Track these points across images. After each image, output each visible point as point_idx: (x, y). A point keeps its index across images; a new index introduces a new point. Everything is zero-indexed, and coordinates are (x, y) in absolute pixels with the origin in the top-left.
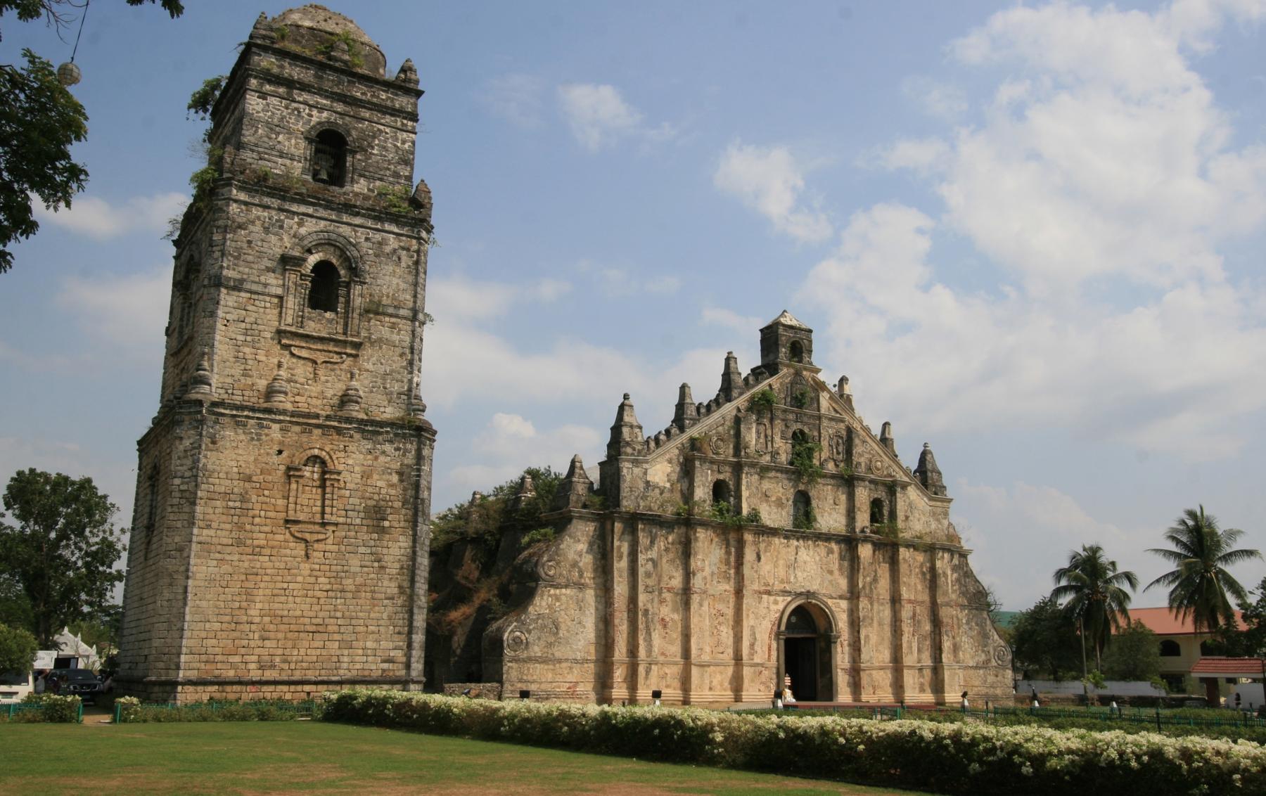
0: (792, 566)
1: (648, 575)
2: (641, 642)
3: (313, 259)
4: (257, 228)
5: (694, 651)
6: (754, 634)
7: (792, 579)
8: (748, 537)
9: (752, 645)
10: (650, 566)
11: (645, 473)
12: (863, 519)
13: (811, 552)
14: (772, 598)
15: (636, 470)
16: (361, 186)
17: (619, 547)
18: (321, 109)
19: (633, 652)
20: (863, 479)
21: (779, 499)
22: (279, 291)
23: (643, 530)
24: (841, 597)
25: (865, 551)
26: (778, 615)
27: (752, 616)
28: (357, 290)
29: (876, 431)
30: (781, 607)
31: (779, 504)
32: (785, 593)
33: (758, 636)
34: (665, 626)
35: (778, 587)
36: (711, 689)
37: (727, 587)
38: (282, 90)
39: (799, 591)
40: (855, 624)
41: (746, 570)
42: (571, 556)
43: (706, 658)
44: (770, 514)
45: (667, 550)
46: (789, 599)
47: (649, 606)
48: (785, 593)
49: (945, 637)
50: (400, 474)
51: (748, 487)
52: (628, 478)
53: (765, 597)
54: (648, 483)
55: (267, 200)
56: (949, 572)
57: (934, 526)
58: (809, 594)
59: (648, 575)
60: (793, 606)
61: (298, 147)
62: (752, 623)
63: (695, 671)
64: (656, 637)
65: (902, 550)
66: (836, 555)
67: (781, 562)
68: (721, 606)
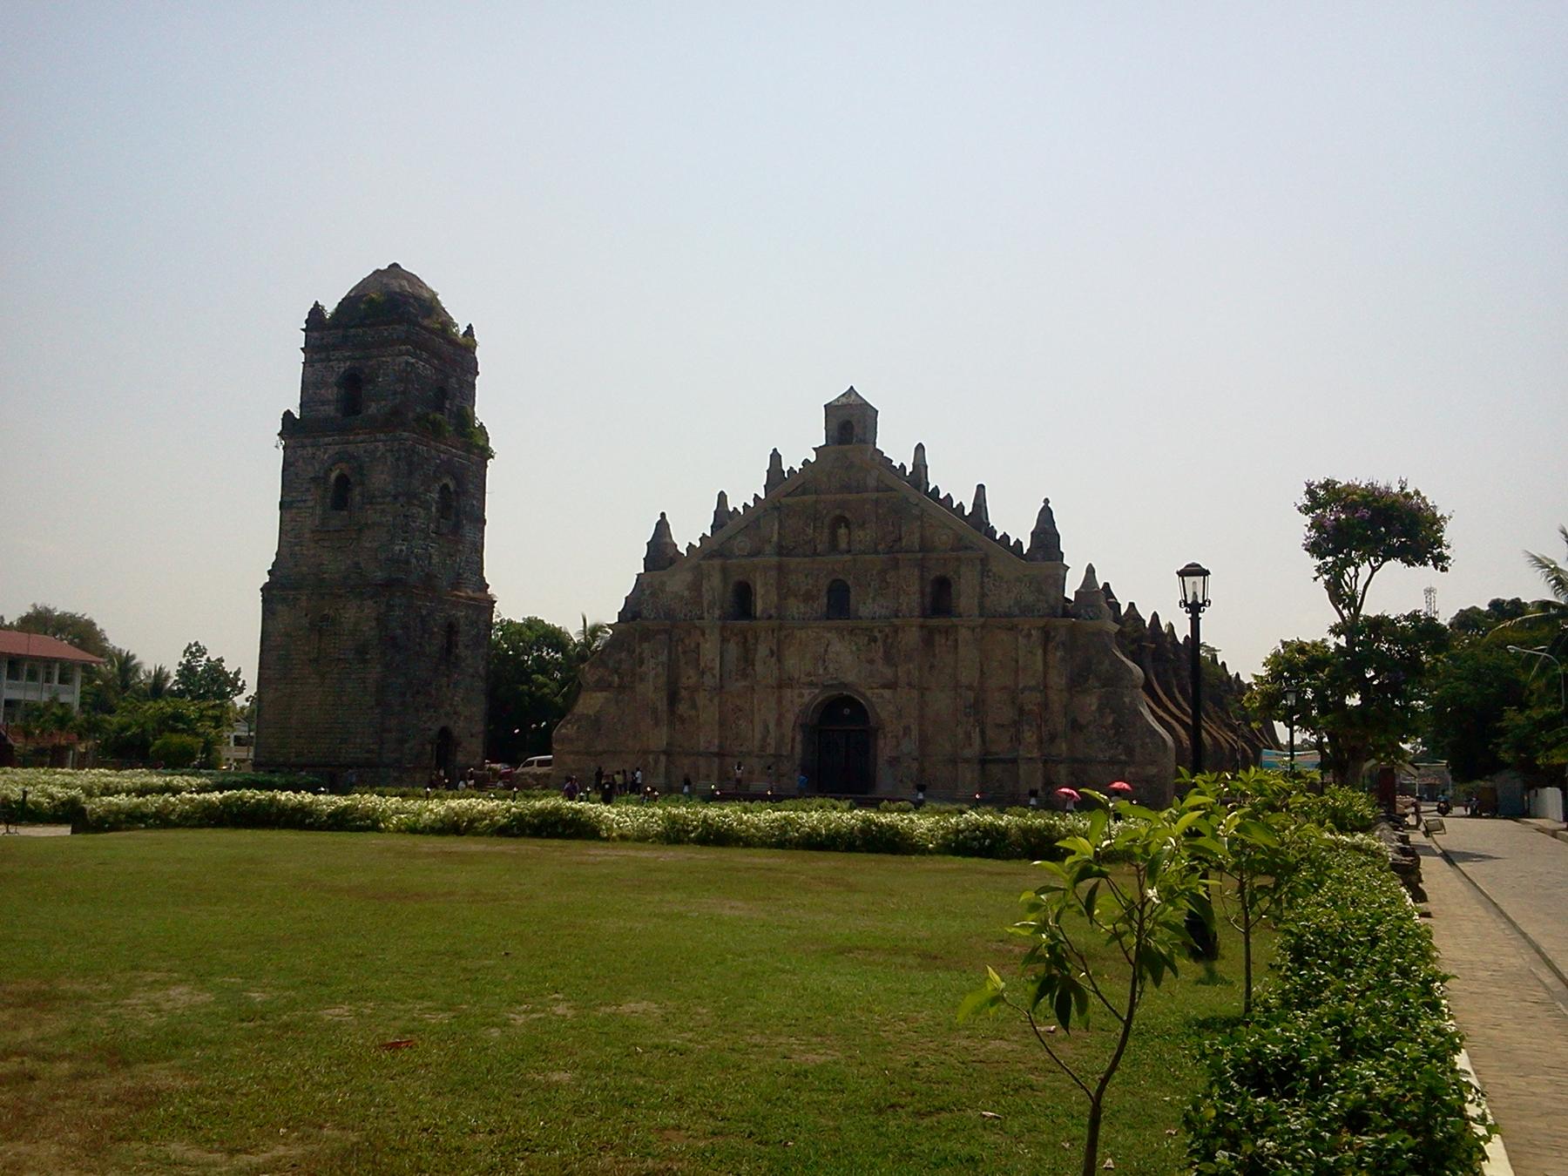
3: (333, 476)
4: (300, 463)
6: (766, 727)
9: (764, 739)
10: (660, 669)
12: (912, 599)
16: (373, 409)
18: (345, 359)
22: (310, 504)
24: (884, 686)
28: (357, 490)
30: (807, 699)
31: (808, 597)
33: (772, 726)
35: (804, 679)
38: (323, 355)
41: (759, 667)
48: (811, 684)
49: (1026, 728)
50: (377, 619)
55: (307, 441)
61: (331, 393)
66: (880, 643)
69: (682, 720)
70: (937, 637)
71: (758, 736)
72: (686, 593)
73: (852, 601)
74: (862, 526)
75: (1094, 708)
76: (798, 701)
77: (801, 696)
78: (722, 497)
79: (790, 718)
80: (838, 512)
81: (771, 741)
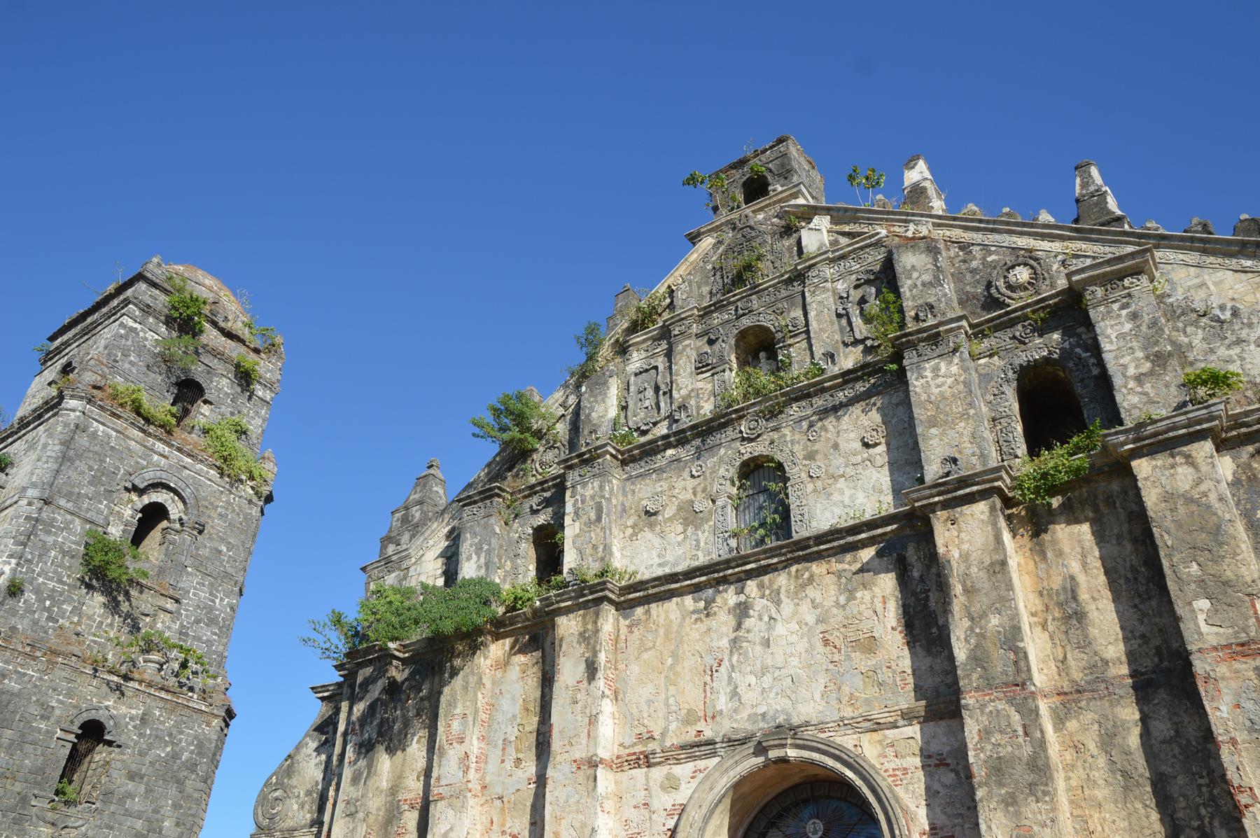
7: (722, 703)
13: (787, 606)
14: (658, 773)
31: (691, 516)
32: (700, 747)
35: (678, 735)
65: (1142, 467)
67: (689, 663)
76: (664, 801)
77: (671, 785)
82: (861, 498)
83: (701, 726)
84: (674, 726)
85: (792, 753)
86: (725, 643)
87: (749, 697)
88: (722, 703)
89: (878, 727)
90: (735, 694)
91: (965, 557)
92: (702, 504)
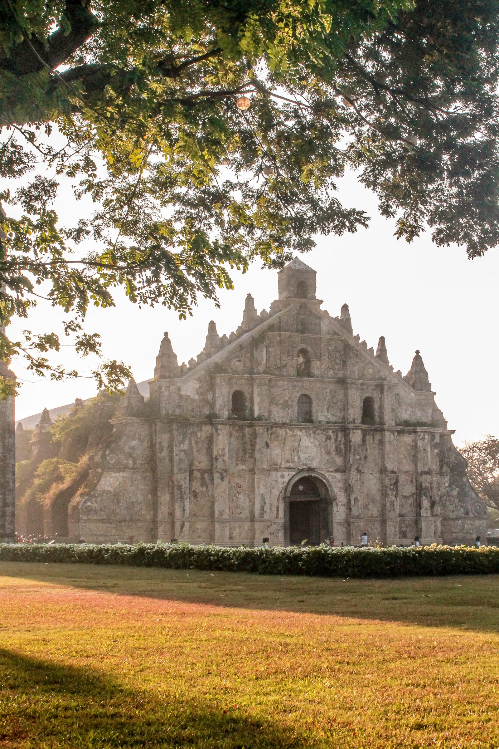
0: (295, 450)
1: (181, 461)
2: (176, 507)
5: (217, 513)
6: (263, 499)
7: (296, 459)
8: (259, 430)
9: (262, 508)
10: (182, 455)
11: (179, 389)
12: (355, 413)
14: (279, 474)
15: (172, 388)
17: (161, 443)
19: (172, 514)
20: (355, 384)
21: (286, 402)
23: (177, 430)
24: (337, 471)
25: (356, 437)
26: (284, 485)
27: (262, 487)
29: (373, 344)
30: (286, 479)
31: (286, 405)
33: (267, 501)
34: (196, 496)
35: (284, 465)
36: (231, 538)
37: (244, 467)
39: (301, 467)
40: (348, 489)
41: (257, 455)
42: (126, 449)
43: (226, 516)
44: (278, 413)
45: (196, 443)
46: (294, 473)
47: (183, 483)
48: (289, 469)
49: (424, 497)
51: (258, 395)
52: (166, 394)
53: (274, 473)
54: (181, 396)
56: (429, 449)
57: (419, 414)
58: (310, 469)
59: (181, 461)
60: (296, 479)
62: (262, 490)
63: (217, 526)
64: (187, 503)
65: (387, 433)
66: (333, 440)
67: (287, 448)
68: (238, 481)
69: (195, 494)
70: (368, 437)
71: (257, 506)
72: (197, 397)
73: (314, 410)
74: (319, 358)
75: (447, 485)
77: (283, 476)
78: (212, 325)
79: (276, 492)
80: (303, 346)
81: (267, 508)
82: (329, 416)
83: (291, 464)
84: (283, 462)
85: (313, 475)
86: (297, 444)
87: (303, 459)
88: (296, 459)
89: (329, 471)
90: (299, 458)
91: (355, 442)
92: (290, 403)
